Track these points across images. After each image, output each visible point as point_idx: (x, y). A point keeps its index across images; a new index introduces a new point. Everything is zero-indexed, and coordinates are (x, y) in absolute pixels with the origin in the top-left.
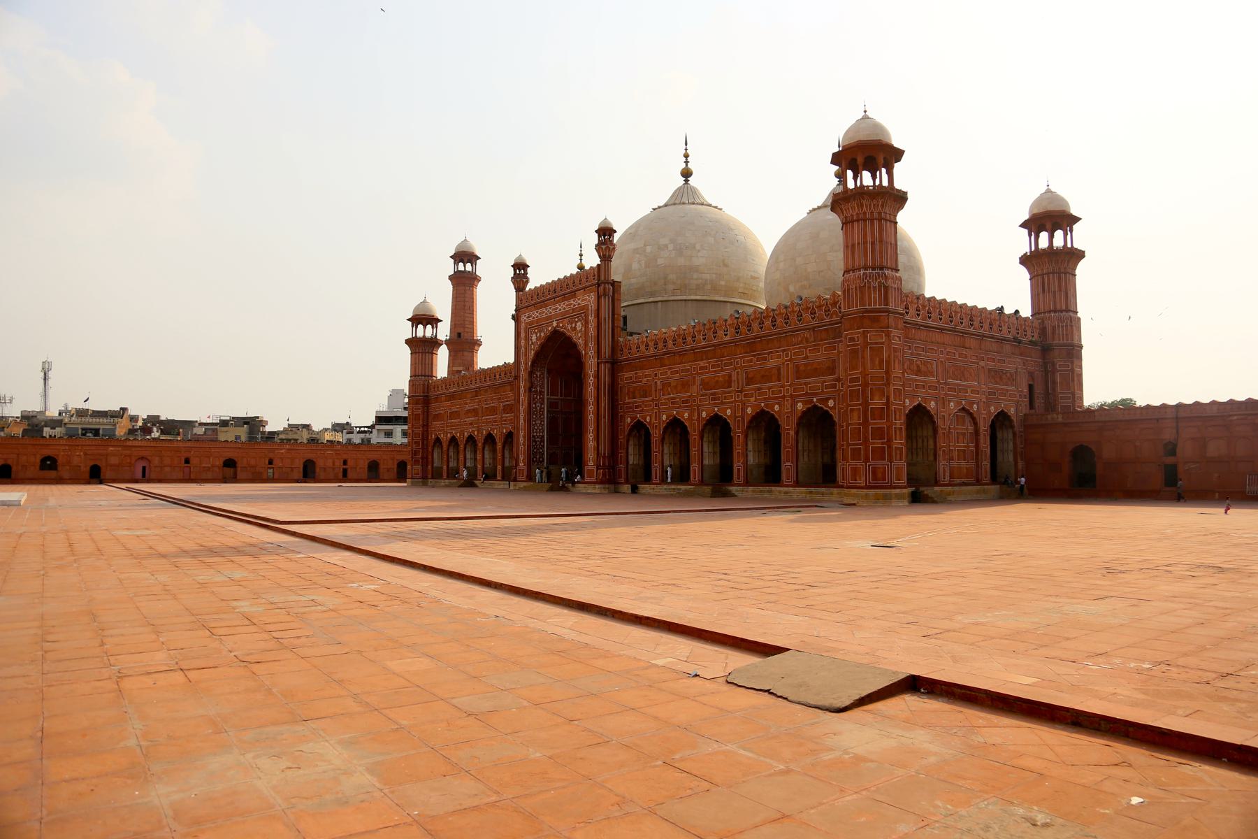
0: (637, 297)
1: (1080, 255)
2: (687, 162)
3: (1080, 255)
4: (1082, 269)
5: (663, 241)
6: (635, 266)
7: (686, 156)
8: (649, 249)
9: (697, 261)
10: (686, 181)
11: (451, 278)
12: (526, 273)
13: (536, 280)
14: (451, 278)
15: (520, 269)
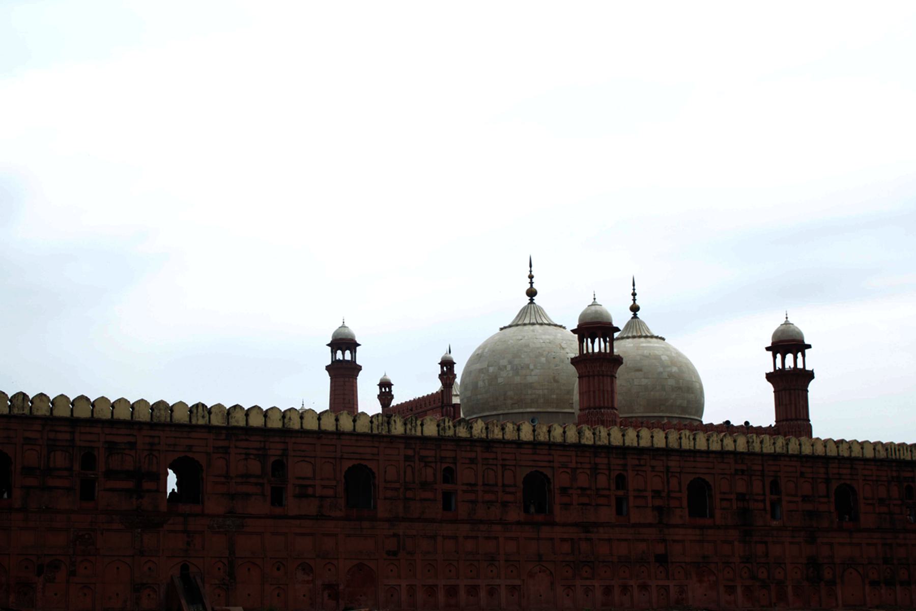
0: (483, 410)
1: (810, 375)
2: (531, 283)
3: (810, 375)
4: (812, 387)
5: (503, 362)
6: (480, 384)
7: (531, 277)
8: (491, 369)
9: (530, 379)
10: (532, 301)
11: (328, 368)
12: (390, 391)
13: (400, 397)
14: (328, 368)
15: (385, 385)
